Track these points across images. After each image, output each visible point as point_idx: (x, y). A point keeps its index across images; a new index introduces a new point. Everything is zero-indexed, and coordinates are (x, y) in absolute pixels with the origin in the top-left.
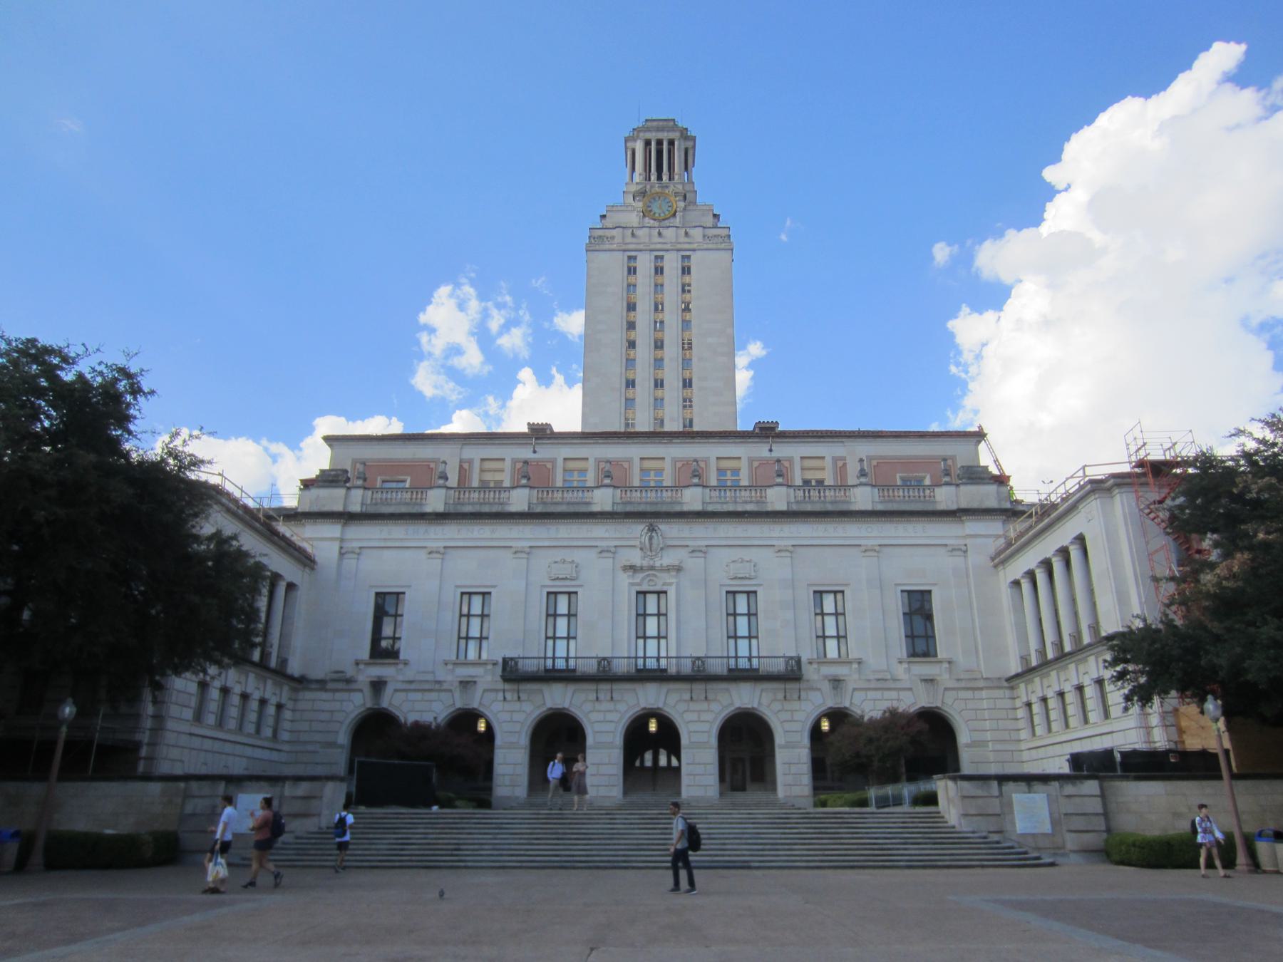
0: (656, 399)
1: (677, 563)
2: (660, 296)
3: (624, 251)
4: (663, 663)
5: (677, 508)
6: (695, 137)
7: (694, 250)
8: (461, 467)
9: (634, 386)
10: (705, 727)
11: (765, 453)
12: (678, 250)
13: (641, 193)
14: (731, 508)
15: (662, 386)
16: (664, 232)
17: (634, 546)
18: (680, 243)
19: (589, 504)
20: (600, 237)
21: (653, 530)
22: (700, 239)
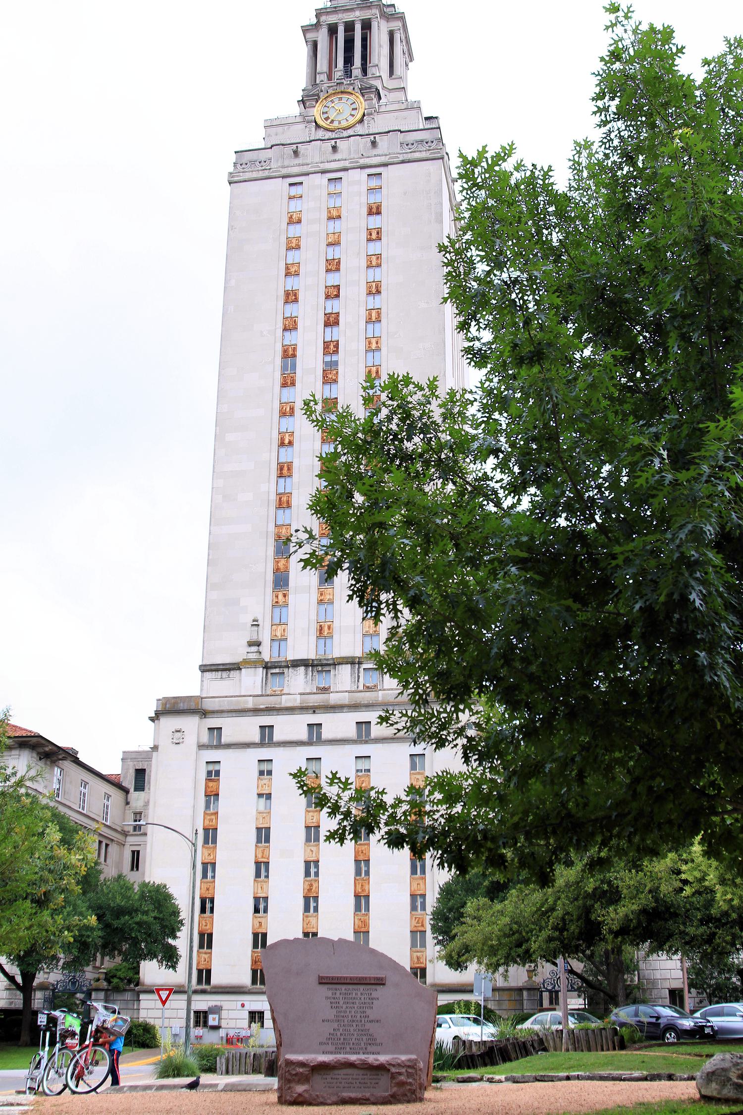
13: (313, 95)
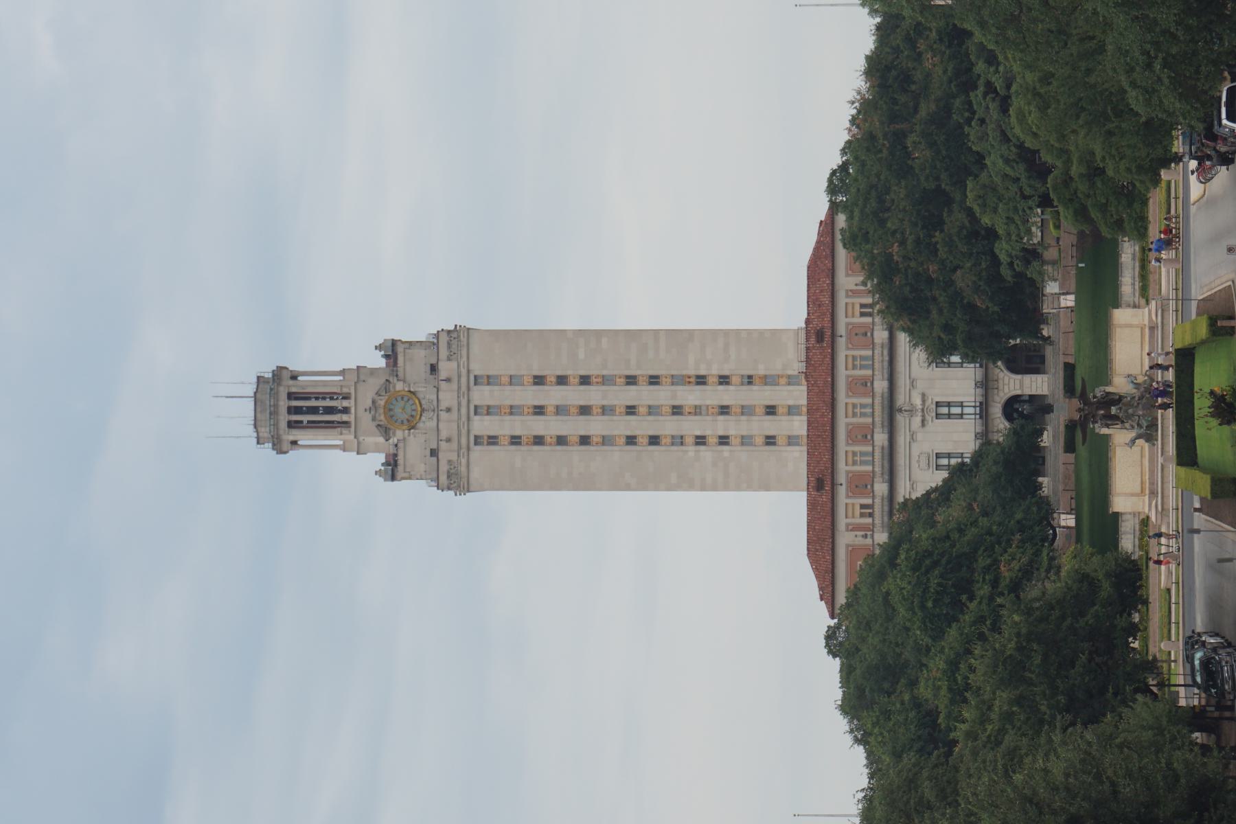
0: (650, 414)
1: (920, 396)
2: (526, 410)
3: (468, 449)
4: (978, 404)
5: (886, 395)
6: (277, 367)
7: (469, 371)
8: (851, 530)
9: (635, 437)
10: (1012, 381)
11: (843, 339)
12: (469, 389)
13: (386, 432)
14: (886, 364)
15: (633, 407)
16: (443, 405)
17: (910, 420)
18: (459, 388)
19: (883, 448)
20: (448, 477)
21: (901, 409)
22: (454, 365)
